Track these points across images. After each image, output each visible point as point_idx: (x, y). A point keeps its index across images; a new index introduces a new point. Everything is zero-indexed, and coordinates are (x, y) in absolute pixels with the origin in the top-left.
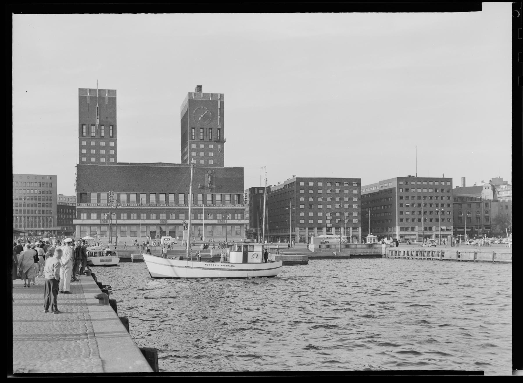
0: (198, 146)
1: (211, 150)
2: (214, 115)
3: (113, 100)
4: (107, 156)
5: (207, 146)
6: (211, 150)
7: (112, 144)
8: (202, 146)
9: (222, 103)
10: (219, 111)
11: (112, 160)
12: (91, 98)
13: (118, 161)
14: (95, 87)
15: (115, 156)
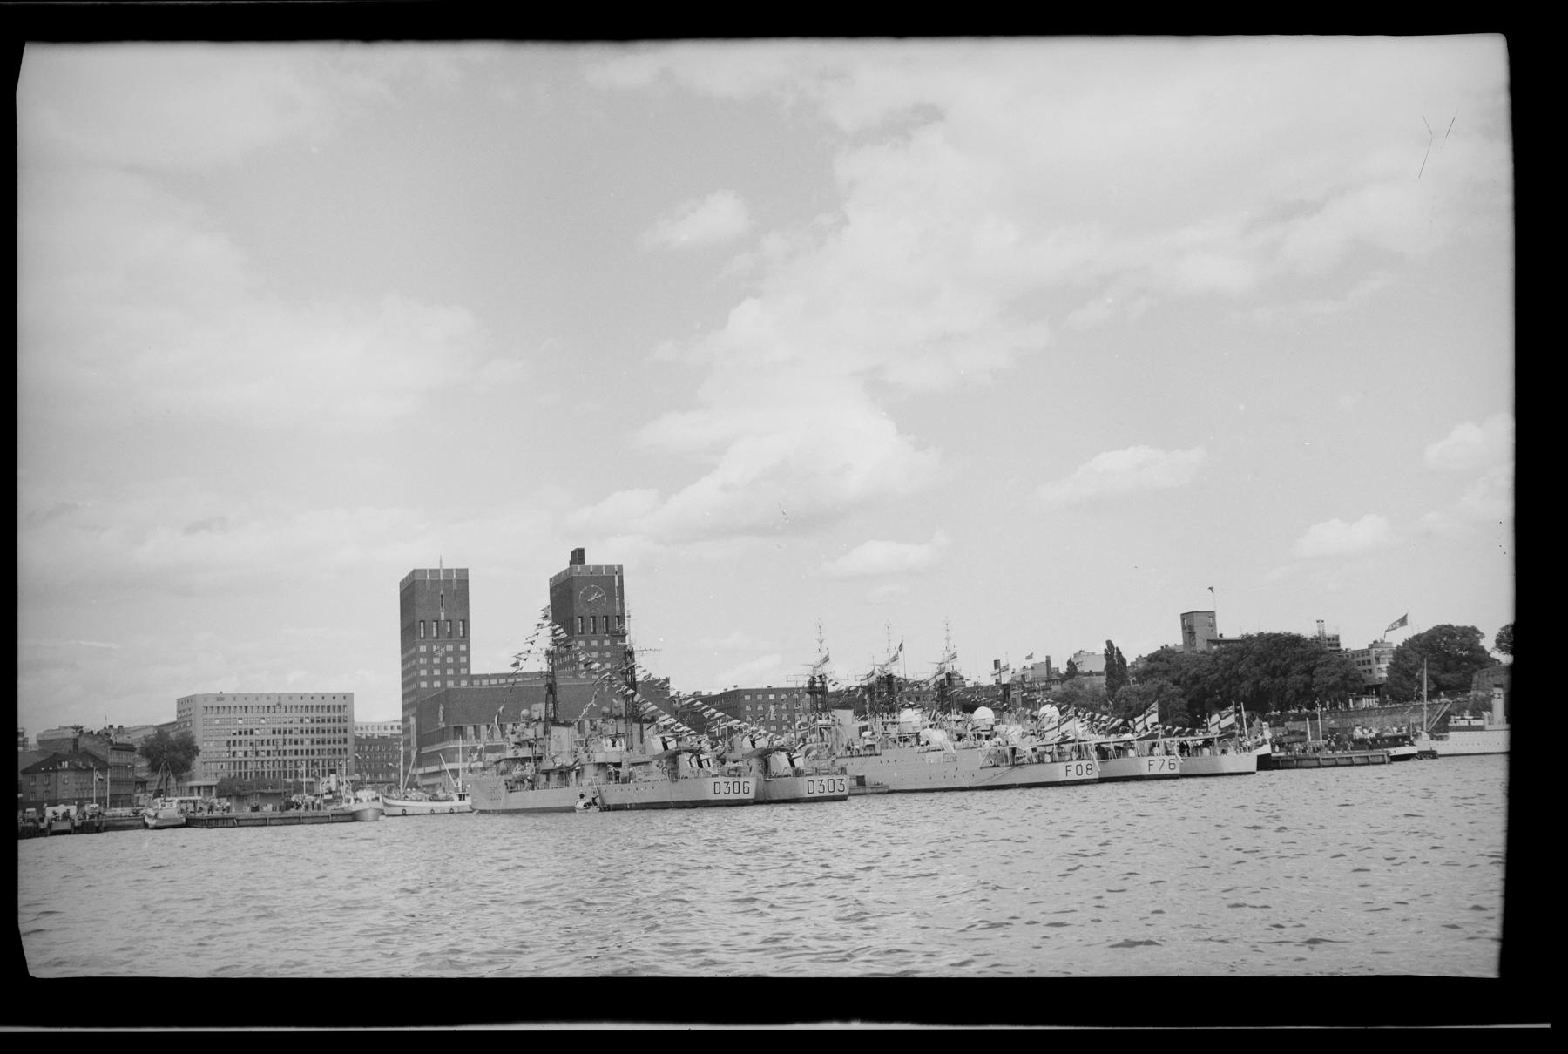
1: (607, 649)
2: (611, 595)
3: (463, 584)
5: (601, 642)
6: (607, 649)
7: (463, 648)
8: (594, 643)
9: (621, 579)
11: (464, 671)
13: (473, 672)
14: (437, 567)
15: (467, 665)
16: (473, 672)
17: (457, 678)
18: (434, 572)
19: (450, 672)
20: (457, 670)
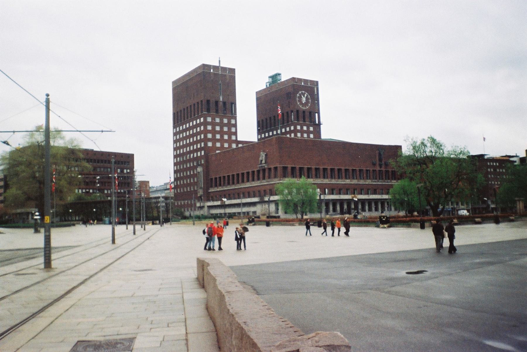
0: (302, 128)
1: (312, 132)
3: (233, 78)
4: (230, 134)
5: (308, 128)
6: (312, 132)
10: (316, 97)
12: (215, 74)
13: (239, 139)
15: (235, 134)
16: (239, 139)
17: (230, 141)
18: (215, 68)
19: (226, 137)
20: (230, 137)
